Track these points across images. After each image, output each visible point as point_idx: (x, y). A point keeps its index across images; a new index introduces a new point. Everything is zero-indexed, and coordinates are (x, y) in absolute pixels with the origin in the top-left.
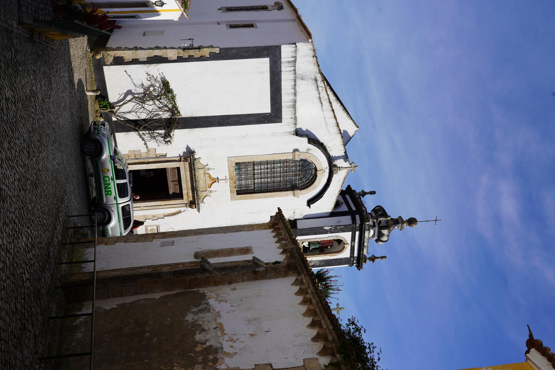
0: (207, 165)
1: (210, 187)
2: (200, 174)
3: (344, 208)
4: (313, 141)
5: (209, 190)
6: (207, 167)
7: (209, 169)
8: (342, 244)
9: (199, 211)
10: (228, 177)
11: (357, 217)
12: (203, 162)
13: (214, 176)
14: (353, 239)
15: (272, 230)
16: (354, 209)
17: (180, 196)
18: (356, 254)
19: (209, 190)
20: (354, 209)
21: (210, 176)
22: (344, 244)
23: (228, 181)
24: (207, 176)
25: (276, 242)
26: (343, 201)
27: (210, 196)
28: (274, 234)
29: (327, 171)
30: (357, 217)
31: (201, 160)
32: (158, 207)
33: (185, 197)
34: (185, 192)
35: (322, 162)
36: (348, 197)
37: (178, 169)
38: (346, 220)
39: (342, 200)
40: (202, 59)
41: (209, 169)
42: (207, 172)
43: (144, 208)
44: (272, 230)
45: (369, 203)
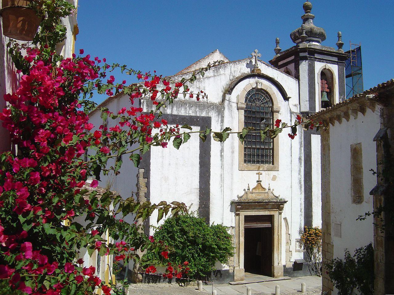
0: (245, 190)
1: (264, 189)
2: (252, 197)
3: (291, 67)
4: (229, 90)
6: (246, 190)
7: (249, 189)
8: (325, 71)
9: (285, 202)
10: (258, 172)
11: (302, 54)
12: (242, 193)
13: (255, 184)
14: (320, 60)
15: (330, 124)
16: (293, 57)
17: (270, 219)
18: (335, 59)
20: (293, 57)
21: (254, 188)
22: (325, 69)
23: (261, 172)
24: (254, 191)
25: (348, 121)
26: (285, 67)
27: (273, 190)
28: (336, 122)
29: (257, 79)
30: (302, 54)
31: (240, 195)
32: (280, 238)
33: (272, 213)
34: (267, 213)
35: (250, 83)
36: (280, 63)
37: (246, 217)
38: (304, 66)
39: (283, 69)
40: (148, 185)
41: (249, 189)
42: (251, 190)
43: (280, 251)
44: (330, 124)
45: (287, 45)
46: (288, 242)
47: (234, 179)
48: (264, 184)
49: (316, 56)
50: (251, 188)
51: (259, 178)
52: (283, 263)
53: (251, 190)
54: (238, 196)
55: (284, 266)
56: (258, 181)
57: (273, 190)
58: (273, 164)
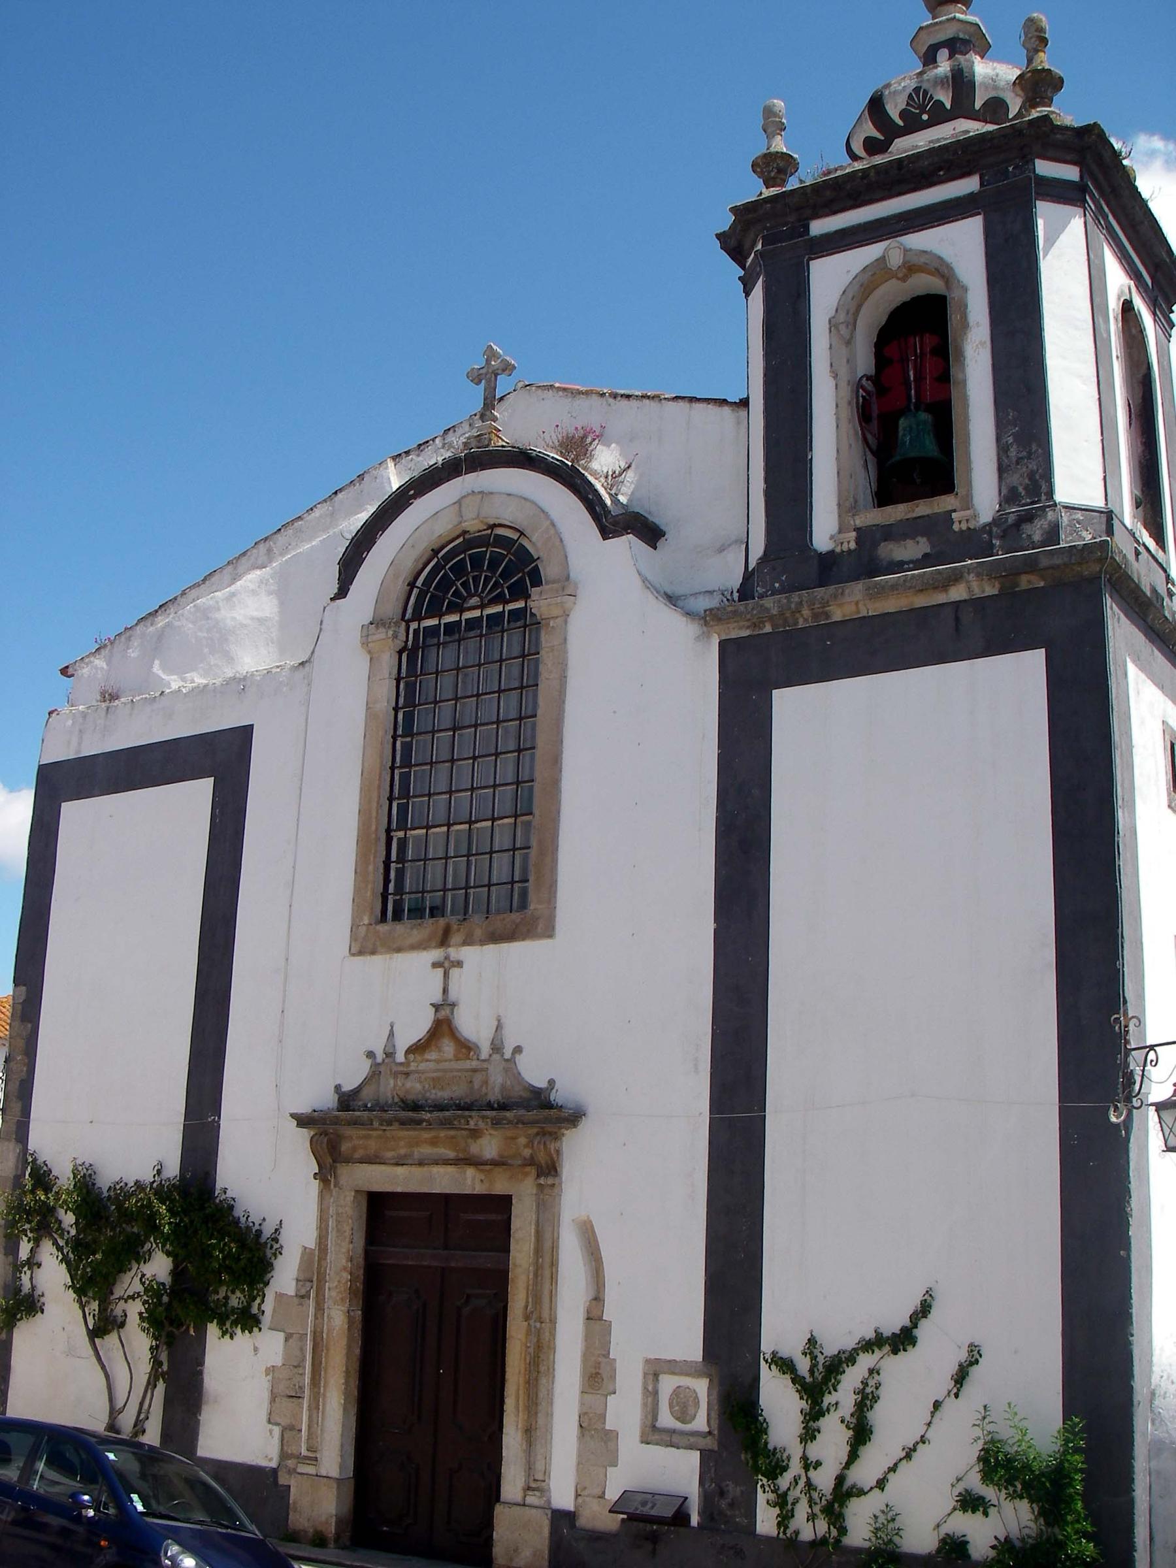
0: (370, 1055)
1: (466, 1048)
5: (485, 1051)
6: (379, 1059)
7: (389, 1055)
10: (436, 954)
12: (353, 1076)
19: (485, 1051)
21: (417, 1049)
23: (454, 953)
27: (518, 1050)
31: (349, 1086)
33: (500, 1186)
34: (470, 1182)
41: (389, 1055)
42: (400, 1057)
46: (597, 1377)
47: (327, 1003)
48: (473, 1024)
49: (819, 227)
50: (403, 1043)
51: (445, 991)
52: (563, 1497)
53: (400, 1057)
54: (338, 1088)
55: (562, 1519)
56: (437, 1007)
57: (518, 1050)
58: (523, 905)
